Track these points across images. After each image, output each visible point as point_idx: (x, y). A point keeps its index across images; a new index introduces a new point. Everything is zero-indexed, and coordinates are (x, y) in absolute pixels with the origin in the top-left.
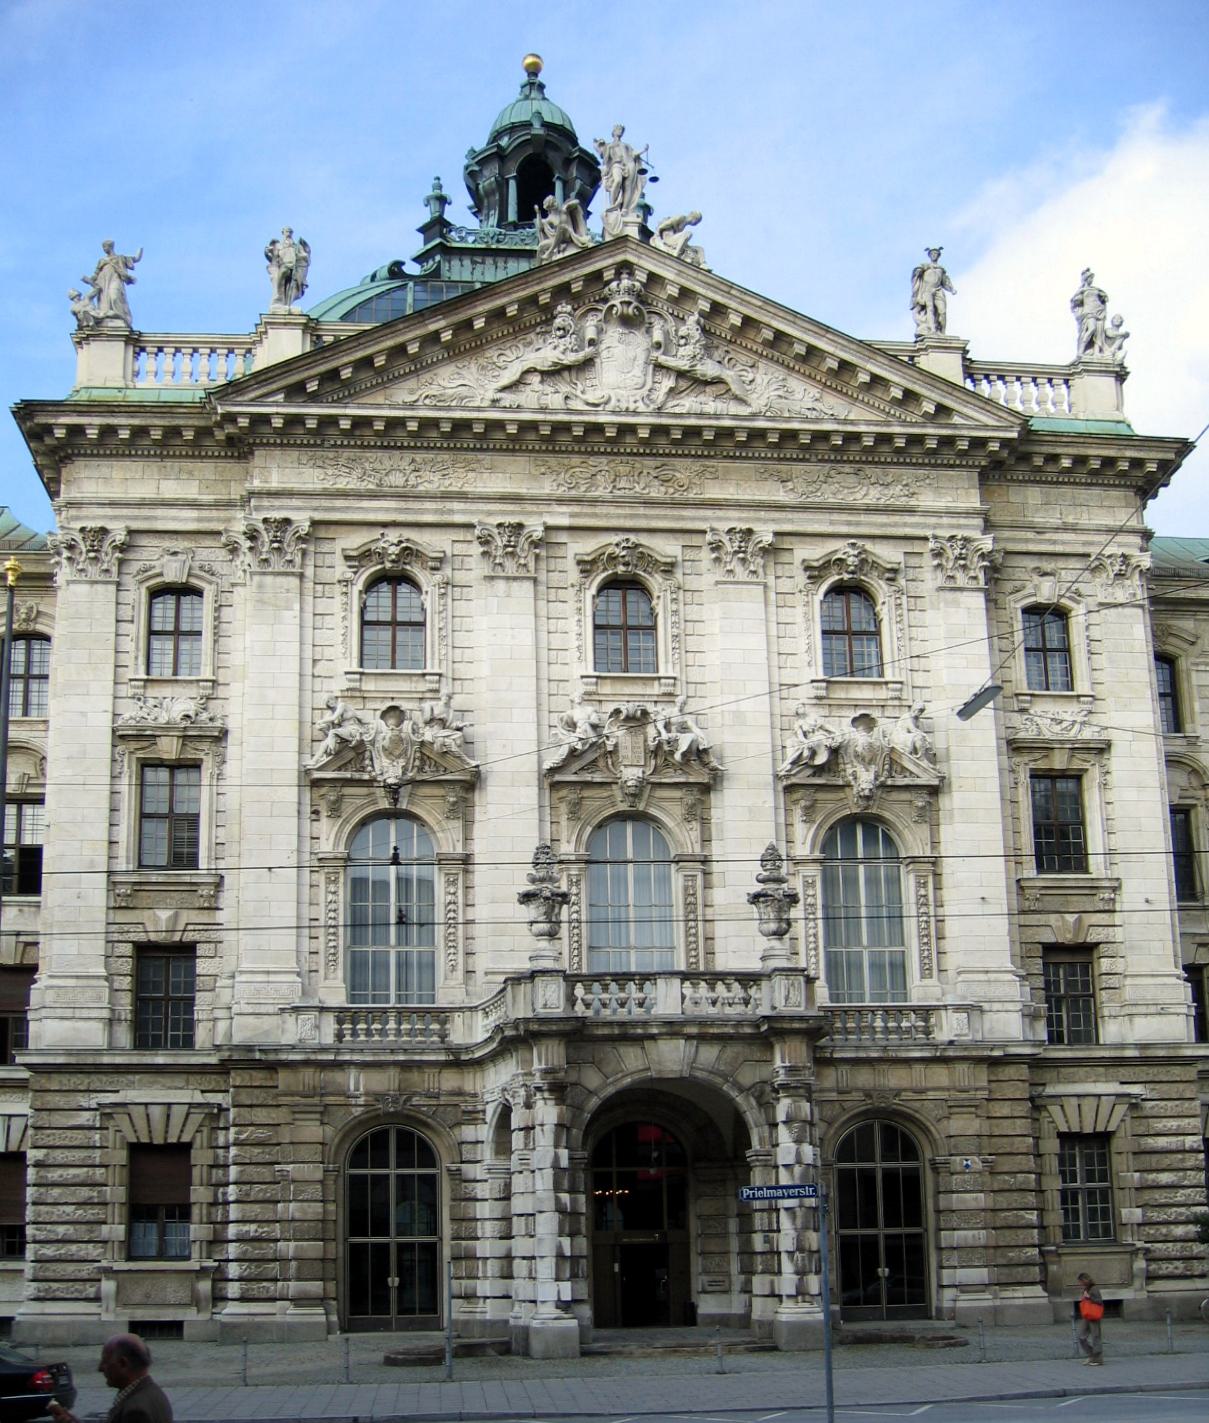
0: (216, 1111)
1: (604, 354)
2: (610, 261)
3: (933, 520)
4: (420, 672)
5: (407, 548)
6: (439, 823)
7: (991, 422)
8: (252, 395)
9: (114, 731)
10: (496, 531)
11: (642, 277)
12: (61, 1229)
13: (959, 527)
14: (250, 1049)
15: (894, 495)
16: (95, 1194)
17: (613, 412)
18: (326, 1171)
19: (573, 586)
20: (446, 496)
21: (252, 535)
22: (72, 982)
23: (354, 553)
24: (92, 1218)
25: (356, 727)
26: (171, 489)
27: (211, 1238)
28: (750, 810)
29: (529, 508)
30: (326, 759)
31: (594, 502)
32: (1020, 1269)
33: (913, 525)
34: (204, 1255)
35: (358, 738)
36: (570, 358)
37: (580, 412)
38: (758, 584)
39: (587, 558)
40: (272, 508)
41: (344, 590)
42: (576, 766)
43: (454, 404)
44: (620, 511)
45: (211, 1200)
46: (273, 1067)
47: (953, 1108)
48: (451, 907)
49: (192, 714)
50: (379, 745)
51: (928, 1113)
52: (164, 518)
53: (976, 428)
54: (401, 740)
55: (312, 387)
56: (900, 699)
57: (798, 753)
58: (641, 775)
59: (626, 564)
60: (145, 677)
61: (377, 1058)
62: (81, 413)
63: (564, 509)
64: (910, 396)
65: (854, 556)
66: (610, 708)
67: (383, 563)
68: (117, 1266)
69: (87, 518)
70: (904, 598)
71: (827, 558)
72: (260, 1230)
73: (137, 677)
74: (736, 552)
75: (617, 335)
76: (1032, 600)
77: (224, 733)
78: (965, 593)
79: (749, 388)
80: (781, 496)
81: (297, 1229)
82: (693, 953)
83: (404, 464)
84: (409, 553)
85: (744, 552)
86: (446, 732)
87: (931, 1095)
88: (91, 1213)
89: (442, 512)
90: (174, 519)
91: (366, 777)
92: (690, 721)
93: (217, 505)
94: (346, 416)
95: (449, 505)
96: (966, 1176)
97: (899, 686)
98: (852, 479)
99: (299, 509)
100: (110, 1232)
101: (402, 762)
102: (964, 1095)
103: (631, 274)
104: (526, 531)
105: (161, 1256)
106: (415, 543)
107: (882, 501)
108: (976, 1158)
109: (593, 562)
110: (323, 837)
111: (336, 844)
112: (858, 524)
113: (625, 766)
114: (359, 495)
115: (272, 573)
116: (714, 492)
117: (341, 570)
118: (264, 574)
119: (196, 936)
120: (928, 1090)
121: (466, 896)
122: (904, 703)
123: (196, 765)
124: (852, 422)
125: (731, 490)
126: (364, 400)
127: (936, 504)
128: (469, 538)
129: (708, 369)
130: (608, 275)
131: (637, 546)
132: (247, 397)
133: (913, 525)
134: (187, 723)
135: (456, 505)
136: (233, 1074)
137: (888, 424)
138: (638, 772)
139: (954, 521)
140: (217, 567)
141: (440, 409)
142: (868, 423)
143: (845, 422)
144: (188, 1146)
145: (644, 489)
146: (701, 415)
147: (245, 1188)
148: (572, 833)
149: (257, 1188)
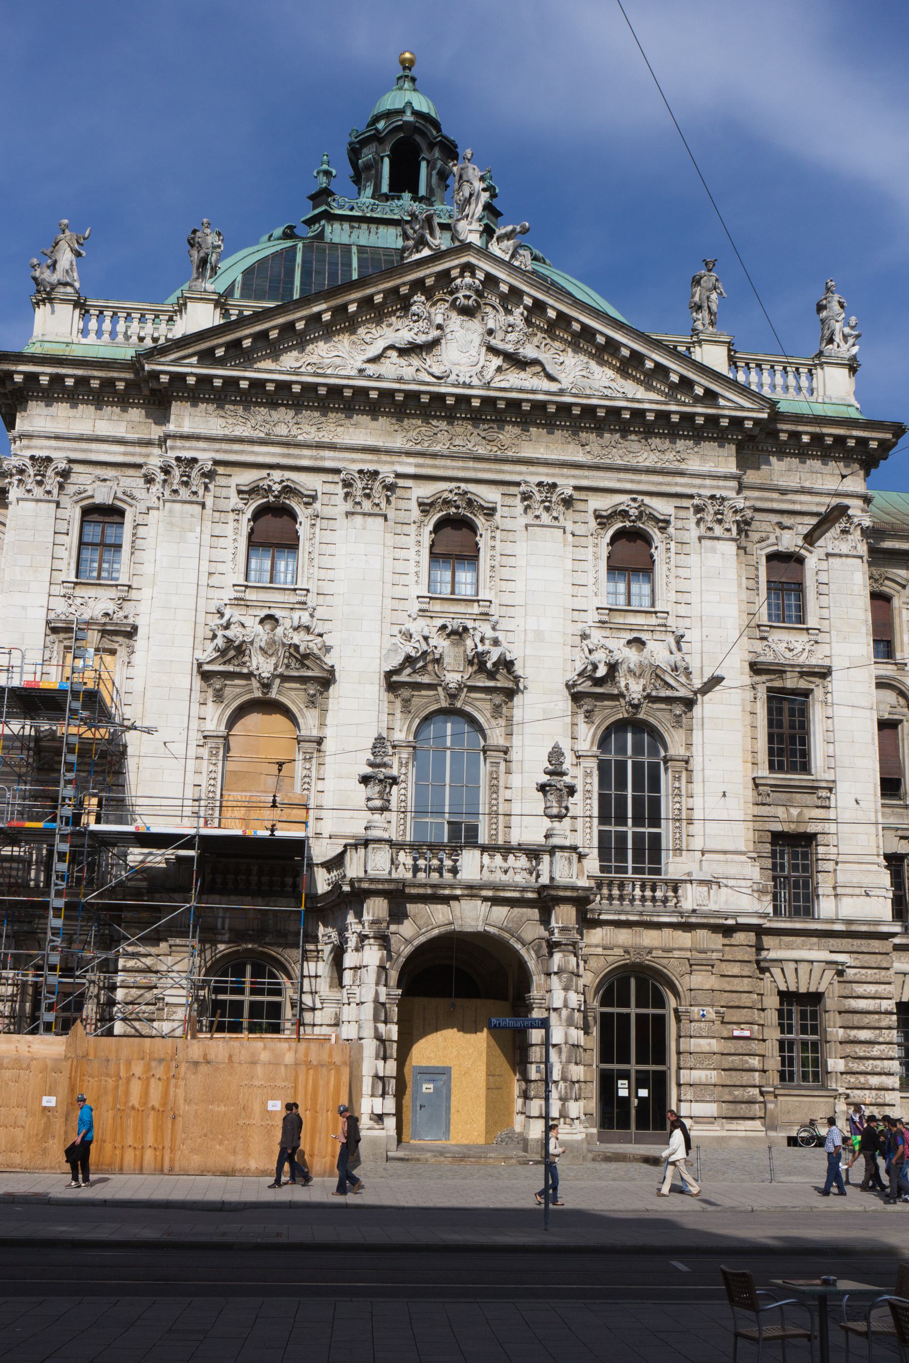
1: (449, 336)
2: (456, 262)
3: (698, 481)
5: (287, 486)
6: (300, 710)
7: (747, 404)
9: (48, 622)
10: (357, 475)
11: (480, 275)
13: (718, 487)
15: (668, 460)
17: (453, 385)
19: (414, 523)
20: (320, 446)
21: (166, 470)
23: (246, 488)
25: (240, 629)
29: (384, 458)
30: (216, 655)
31: (434, 456)
32: (743, 1106)
33: (682, 485)
35: (241, 639)
36: (421, 339)
37: (428, 384)
38: (559, 527)
39: (426, 501)
40: (183, 448)
41: (237, 517)
42: (408, 671)
43: (329, 371)
47: (692, 965)
48: (307, 780)
49: (111, 612)
50: (256, 645)
51: (673, 968)
52: (98, 452)
53: (735, 409)
54: (274, 642)
55: (220, 352)
56: (665, 626)
57: (583, 667)
58: (460, 679)
59: (457, 507)
60: (75, 580)
63: (411, 460)
64: (686, 384)
65: (636, 508)
66: (439, 623)
67: (268, 497)
69: (36, 447)
70: (673, 544)
71: (614, 509)
73: (69, 580)
74: (543, 502)
75: (459, 322)
76: (775, 548)
77: (135, 628)
78: (721, 542)
79: (560, 368)
80: (580, 456)
82: (494, 826)
84: (289, 490)
85: (550, 501)
87: (676, 954)
89: (316, 459)
90: (106, 452)
91: (245, 671)
92: (501, 636)
94: (245, 378)
96: (702, 1024)
97: (666, 615)
98: (636, 446)
99: (204, 450)
101: (273, 660)
102: (703, 956)
103: (473, 275)
104: (380, 476)
106: (293, 481)
107: (659, 465)
108: (711, 1010)
109: (432, 504)
110: (208, 719)
111: (219, 724)
112: (639, 482)
114: (251, 442)
116: (528, 452)
117: (235, 501)
118: (174, 501)
120: (674, 949)
121: (318, 771)
122: (669, 629)
124: (639, 401)
125: (542, 451)
126: (258, 365)
127: (701, 468)
128: (336, 480)
129: (529, 352)
130: (455, 273)
131: (466, 493)
133: (682, 485)
134: (107, 620)
135: (327, 453)
137: (666, 404)
138: (457, 677)
139: (715, 483)
140: (136, 493)
143: (633, 400)
145: (474, 446)
146: (521, 390)
148: (404, 723)
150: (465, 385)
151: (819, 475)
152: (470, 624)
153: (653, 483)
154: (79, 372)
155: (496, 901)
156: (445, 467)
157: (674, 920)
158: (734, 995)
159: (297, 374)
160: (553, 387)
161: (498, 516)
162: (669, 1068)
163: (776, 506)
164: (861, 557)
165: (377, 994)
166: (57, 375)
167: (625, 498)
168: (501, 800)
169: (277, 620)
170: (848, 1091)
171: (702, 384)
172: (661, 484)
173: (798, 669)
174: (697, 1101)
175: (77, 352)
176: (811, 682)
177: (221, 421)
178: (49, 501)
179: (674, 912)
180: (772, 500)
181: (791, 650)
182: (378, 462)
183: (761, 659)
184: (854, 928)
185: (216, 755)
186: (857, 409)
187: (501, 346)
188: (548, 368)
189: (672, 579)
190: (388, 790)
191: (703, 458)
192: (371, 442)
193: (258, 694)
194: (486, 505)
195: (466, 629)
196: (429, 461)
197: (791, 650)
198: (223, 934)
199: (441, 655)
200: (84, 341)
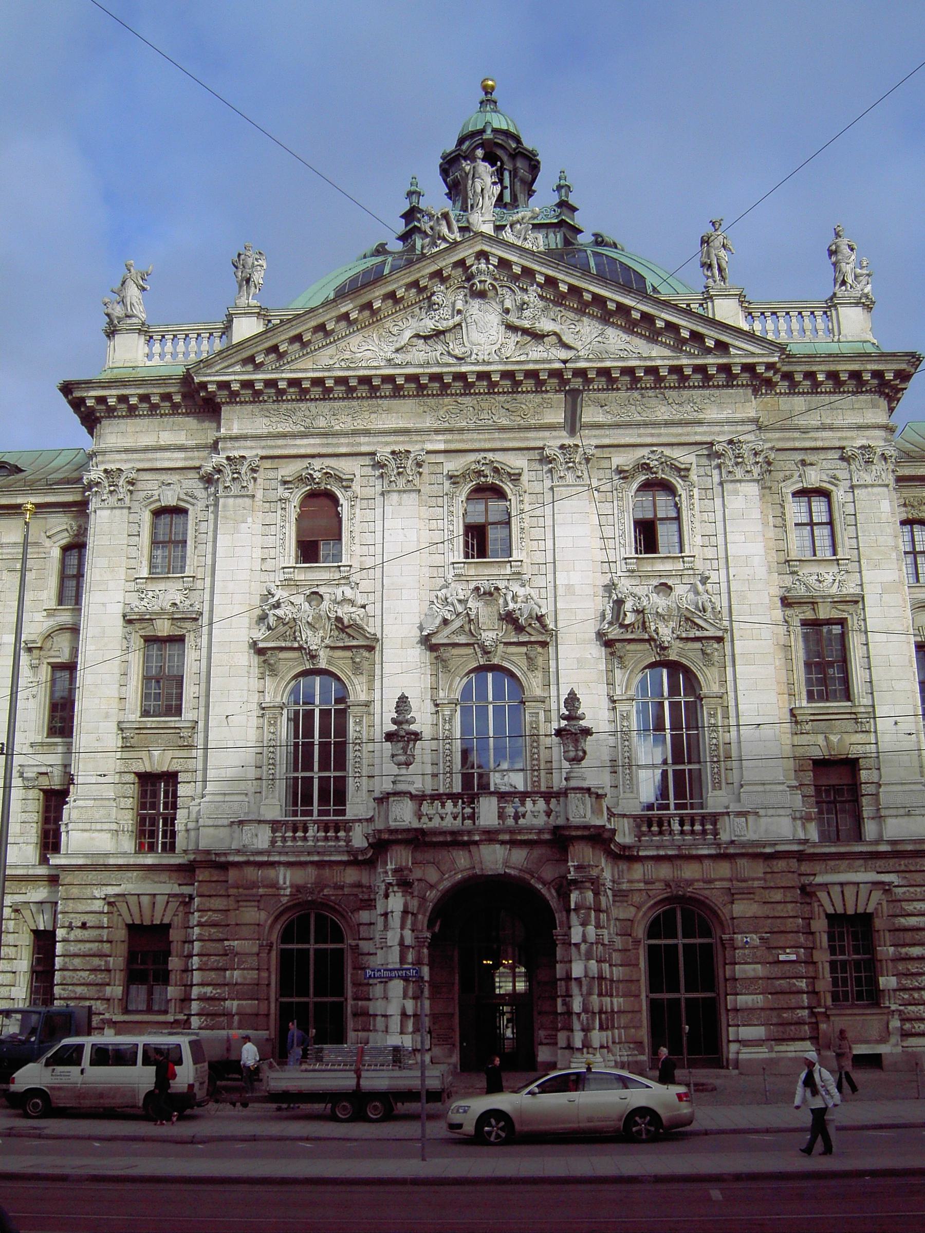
0: (187, 900)
2: (471, 251)
3: (717, 429)
4: (336, 564)
5: (327, 473)
6: (349, 678)
7: (757, 351)
9: (124, 616)
10: (391, 457)
12: (79, 990)
14: (208, 852)
15: (687, 411)
16: (103, 963)
18: (261, 946)
19: (447, 494)
22: (91, 803)
23: (290, 479)
24: (100, 981)
25: (289, 608)
26: (167, 438)
27: (182, 997)
28: (579, 660)
29: (415, 438)
31: (461, 430)
33: (701, 434)
34: (178, 1010)
37: (449, 365)
40: (234, 448)
44: (481, 437)
45: (183, 968)
46: (225, 867)
47: (731, 895)
49: (178, 602)
51: (716, 898)
52: (161, 459)
53: (746, 356)
54: (320, 616)
56: (692, 569)
61: (298, 859)
63: (440, 437)
66: (472, 586)
68: (116, 1018)
69: (109, 462)
72: (214, 992)
75: (477, 306)
78: (743, 484)
81: (239, 991)
83: (326, 411)
85: (574, 462)
86: (354, 609)
87: (718, 884)
88: (100, 977)
89: (353, 445)
90: (169, 459)
93: (198, 447)
94: (283, 379)
95: (357, 439)
96: (746, 951)
98: (653, 402)
99: (251, 448)
100: (112, 992)
102: (744, 885)
104: (412, 455)
105: (149, 1010)
106: (333, 468)
108: (755, 936)
109: (463, 475)
112: (659, 435)
113: (484, 630)
114: (294, 436)
118: (227, 497)
120: (716, 880)
122: (697, 572)
123: (181, 639)
127: (719, 416)
129: (546, 325)
132: (214, 370)
133: (701, 434)
134: (175, 609)
135: (363, 439)
136: (197, 871)
137: (678, 358)
139: (733, 428)
141: (349, 368)
142: (663, 358)
143: (645, 359)
144: (169, 926)
147: (205, 959)
149: (213, 958)
150: (484, 362)
152: (501, 585)
155: (513, 843)
157: (713, 852)
158: (779, 921)
159: (329, 370)
161: (524, 478)
162: (718, 995)
163: (797, 444)
164: (887, 486)
165: (402, 938)
166: (123, 395)
167: (645, 451)
168: (542, 748)
169: (321, 596)
170: (902, 1008)
171: (711, 336)
172: (680, 435)
174: (744, 1025)
175: (142, 374)
177: (265, 420)
178: (122, 508)
179: (712, 844)
180: (794, 439)
181: (820, 582)
182: (410, 442)
183: (793, 593)
184: (900, 848)
186: (873, 344)
187: (517, 323)
188: (564, 338)
189: (697, 524)
190: (411, 746)
191: (721, 406)
192: (402, 424)
193: (308, 666)
194: (512, 471)
195: (497, 589)
196: (456, 437)
197: (820, 582)
198: (285, 889)
199: (477, 615)
200: (149, 363)
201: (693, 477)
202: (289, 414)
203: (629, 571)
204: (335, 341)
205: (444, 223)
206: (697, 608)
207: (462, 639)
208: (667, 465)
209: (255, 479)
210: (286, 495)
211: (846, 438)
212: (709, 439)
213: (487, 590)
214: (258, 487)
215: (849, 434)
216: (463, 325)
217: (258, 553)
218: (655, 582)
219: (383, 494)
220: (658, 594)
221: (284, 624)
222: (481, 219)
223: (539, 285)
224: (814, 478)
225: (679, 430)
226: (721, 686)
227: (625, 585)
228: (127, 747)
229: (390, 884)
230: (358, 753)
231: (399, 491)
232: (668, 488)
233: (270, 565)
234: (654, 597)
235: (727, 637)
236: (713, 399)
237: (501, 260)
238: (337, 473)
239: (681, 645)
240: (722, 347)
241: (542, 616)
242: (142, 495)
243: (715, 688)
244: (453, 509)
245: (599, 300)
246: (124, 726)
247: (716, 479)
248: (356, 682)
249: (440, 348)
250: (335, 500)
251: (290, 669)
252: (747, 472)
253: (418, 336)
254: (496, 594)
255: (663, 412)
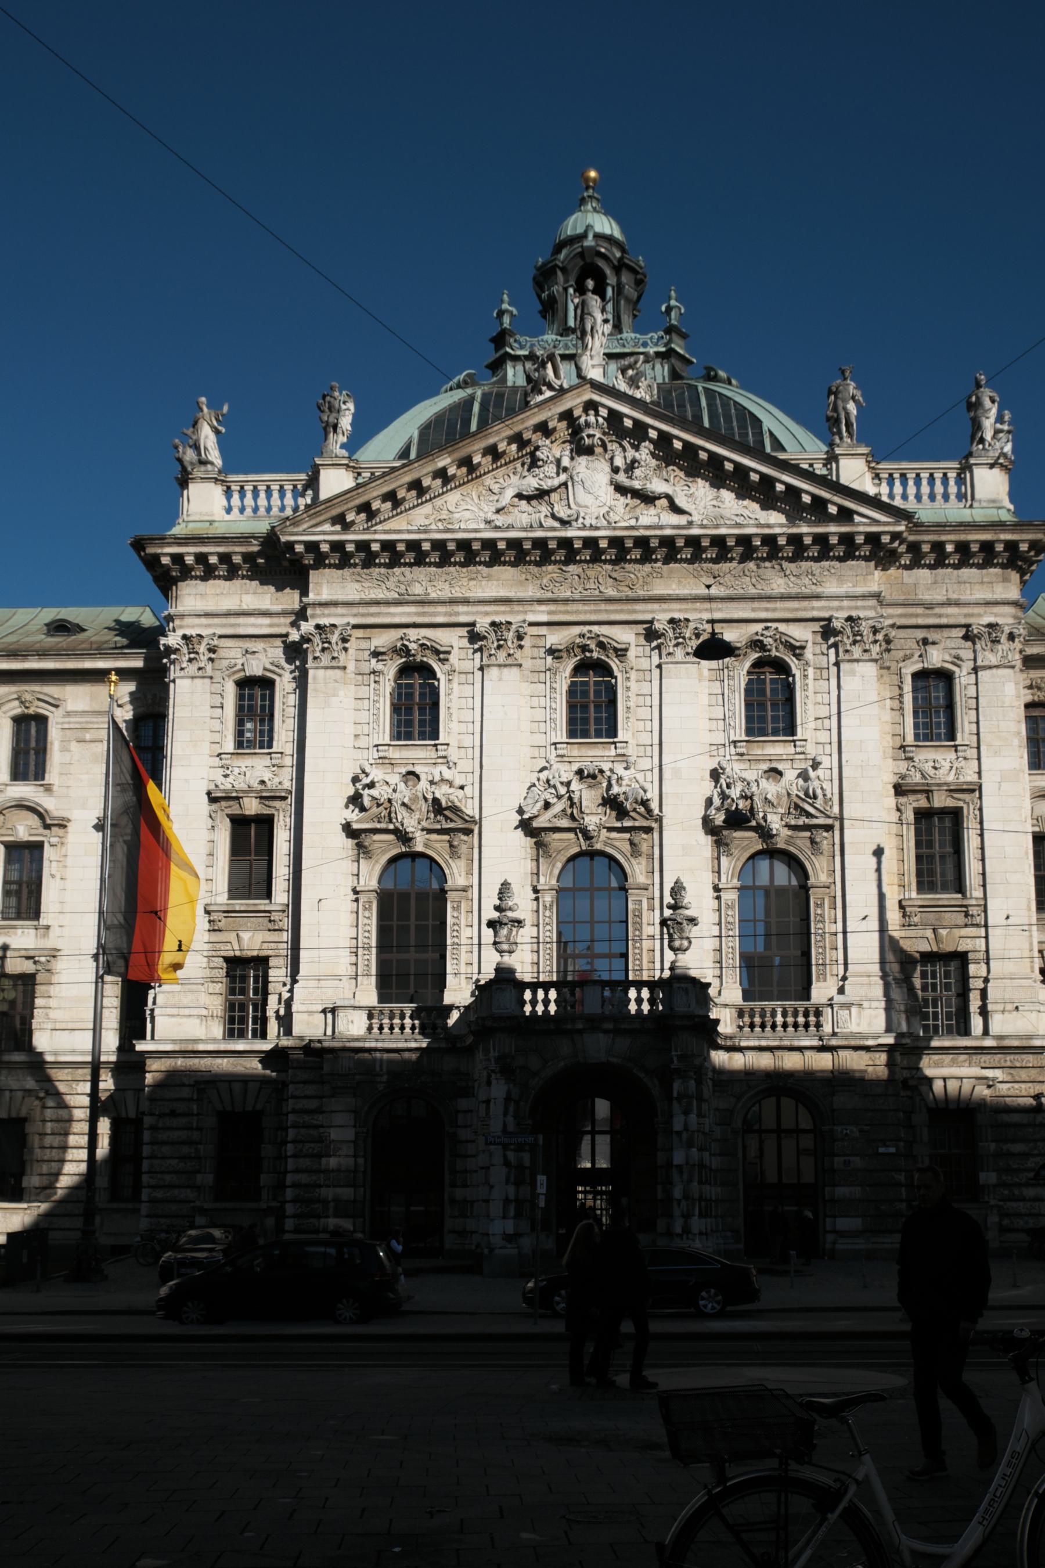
3: (836, 604)
6: (446, 862)
8: (305, 526)
9: (209, 793)
12: (168, 1178)
13: (857, 608)
17: (579, 529)
18: (356, 1133)
19: (549, 670)
20: (453, 602)
29: (517, 608)
31: (566, 601)
37: (553, 529)
40: (324, 615)
44: (586, 608)
48: (456, 928)
49: (266, 779)
54: (417, 797)
56: (803, 753)
62: (180, 544)
63: (543, 608)
64: (819, 504)
66: (575, 767)
68: (206, 1206)
69: (188, 626)
78: (861, 664)
82: (638, 962)
83: (422, 577)
85: (684, 638)
86: (452, 790)
89: (451, 615)
90: (253, 625)
93: (284, 613)
94: (376, 541)
99: (343, 615)
106: (429, 639)
112: (774, 610)
114: (388, 603)
115: (322, 668)
116: (659, 590)
118: (317, 668)
119: (270, 953)
124: (769, 526)
125: (674, 586)
129: (657, 486)
132: (301, 529)
134: (263, 787)
135: (461, 608)
139: (853, 603)
150: (592, 527)
151: (968, 585)
152: (606, 767)
153: (788, 610)
154: (221, 549)
156: (577, 612)
160: (682, 520)
161: (631, 654)
163: (920, 621)
164: (1013, 667)
167: (759, 627)
170: (1001, 1203)
171: (835, 503)
172: (797, 610)
173: (945, 788)
174: (842, 1216)
175: (220, 530)
176: (959, 800)
177: (357, 586)
180: (917, 616)
181: (935, 768)
182: (511, 612)
183: (908, 780)
185: (370, 909)
186: (1009, 510)
191: (841, 579)
195: (601, 771)
196: (561, 607)
197: (935, 768)
200: (227, 517)
201: (808, 654)
202: (382, 580)
203: (738, 754)
204: (431, 499)
205: (549, 365)
206: (807, 794)
207: (565, 823)
208: (781, 642)
209: (346, 649)
210: (379, 666)
211: (971, 615)
212: (826, 615)
213: (591, 771)
214: (349, 657)
215: (977, 610)
216: (570, 484)
217: (351, 730)
218: (765, 766)
219: (481, 669)
220: (768, 779)
221: (379, 805)
222: (590, 363)
223: (651, 441)
224: (936, 658)
225: (795, 604)
226: (829, 875)
227: (735, 769)
228: (214, 930)
229: (493, 1071)
230: (456, 940)
231: (500, 666)
232: (781, 667)
233: (363, 742)
234: (763, 783)
235: (837, 824)
236: (833, 571)
237: (611, 411)
238: (434, 644)
239: (790, 833)
240: (845, 515)
241: (648, 800)
242: (225, 663)
243: (823, 878)
244: (557, 686)
245: (716, 461)
246: (209, 908)
247: (832, 659)
248: (453, 865)
249: (544, 509)
250: (431, 673)
251: (384, 852)
252: (865, 651)
253: (520, 496)
254: (600, 777)
255: (778, 584)
